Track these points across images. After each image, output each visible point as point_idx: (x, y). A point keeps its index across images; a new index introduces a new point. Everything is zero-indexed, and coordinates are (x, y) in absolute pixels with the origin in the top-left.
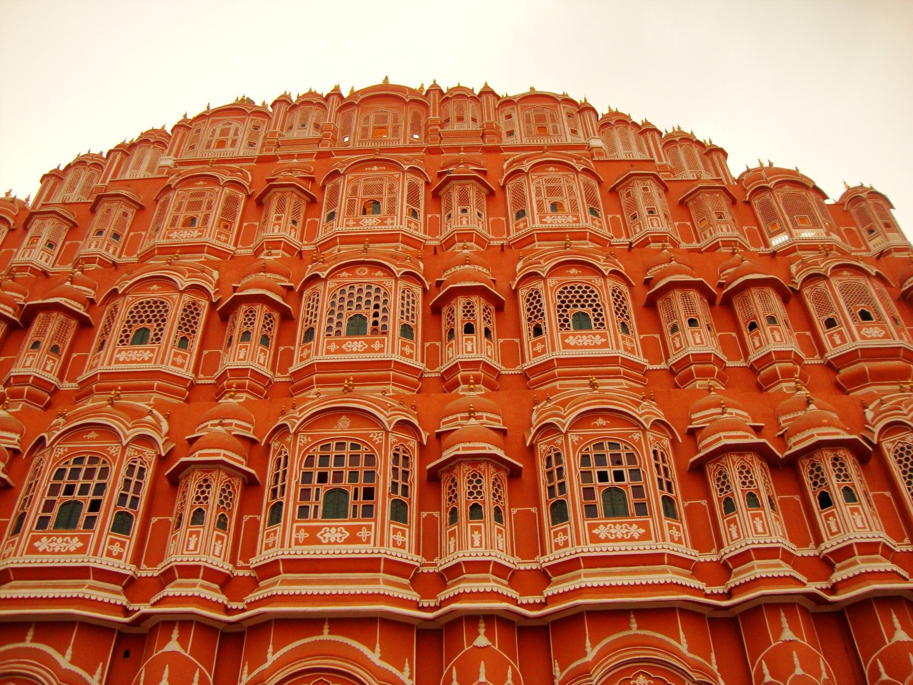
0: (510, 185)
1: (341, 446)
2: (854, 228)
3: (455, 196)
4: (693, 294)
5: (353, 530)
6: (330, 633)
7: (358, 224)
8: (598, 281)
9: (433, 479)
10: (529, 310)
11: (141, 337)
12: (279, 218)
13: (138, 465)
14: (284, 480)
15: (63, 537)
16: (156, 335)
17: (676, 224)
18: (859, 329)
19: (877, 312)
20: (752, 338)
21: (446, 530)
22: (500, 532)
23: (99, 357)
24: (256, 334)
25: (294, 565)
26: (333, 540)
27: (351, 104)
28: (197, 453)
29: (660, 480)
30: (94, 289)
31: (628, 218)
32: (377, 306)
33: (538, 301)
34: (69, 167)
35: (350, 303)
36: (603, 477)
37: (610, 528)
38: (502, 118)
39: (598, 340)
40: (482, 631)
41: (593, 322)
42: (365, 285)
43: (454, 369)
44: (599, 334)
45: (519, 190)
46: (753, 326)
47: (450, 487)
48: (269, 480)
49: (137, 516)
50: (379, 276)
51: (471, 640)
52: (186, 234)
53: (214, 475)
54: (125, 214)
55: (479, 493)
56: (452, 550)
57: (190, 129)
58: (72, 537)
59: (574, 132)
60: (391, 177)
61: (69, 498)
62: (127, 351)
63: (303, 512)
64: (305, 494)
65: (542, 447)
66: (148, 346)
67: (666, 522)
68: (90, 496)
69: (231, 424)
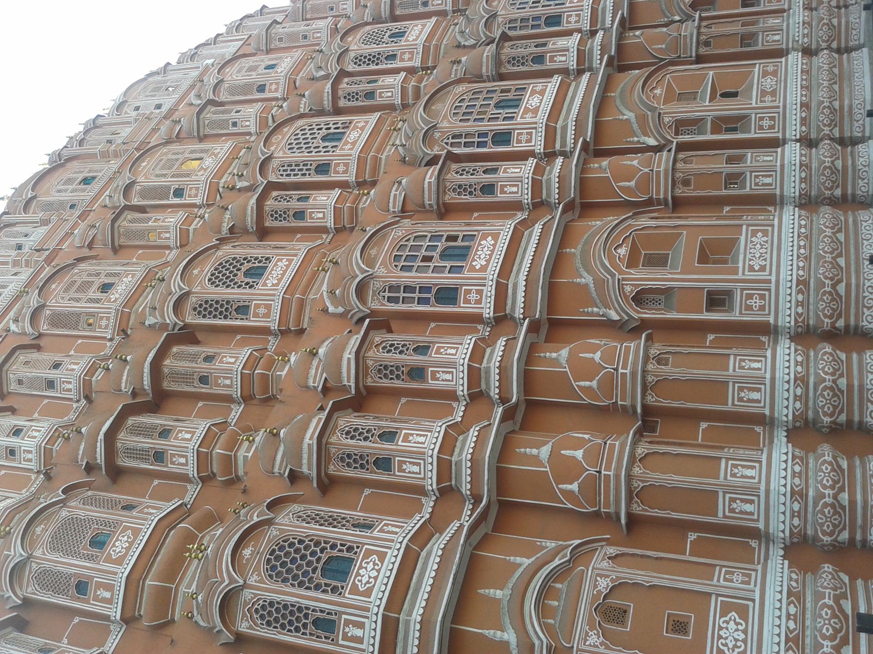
5: (533, 92)
7: (205, 170)
10: (368, 64)
16: (259, 262)
21: (549, 65)
23: (257, 306)
28: (427, 180)
31: (302, 42)
32: (319, 129)
43: (404, 90)
47: (513, 65)
51: (637, 37)
56: (564, 59)
58: (479, 244)
60: (166, 154)
62: (267, 279)
66: (271, 265)
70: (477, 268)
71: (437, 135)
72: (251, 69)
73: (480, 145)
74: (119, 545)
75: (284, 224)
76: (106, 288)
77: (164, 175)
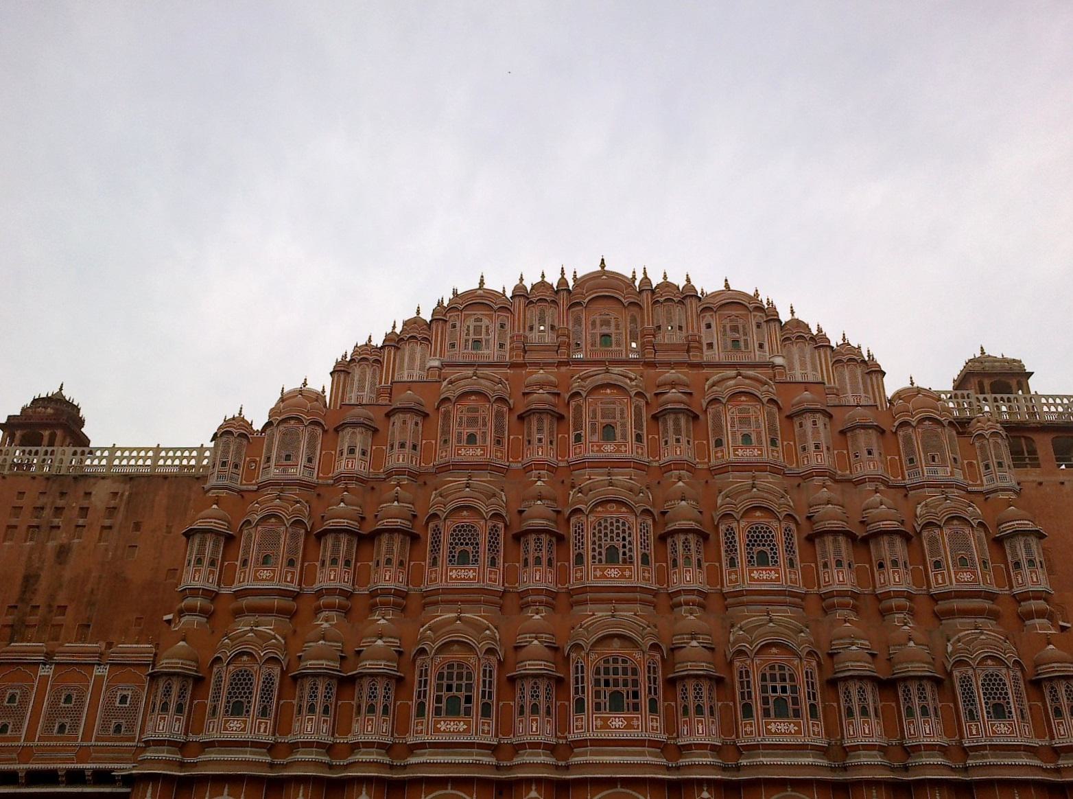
0: (710, 410)
1: (615, 661)
2: (975, 462)
3: (670, 423)
4: (841, 538)
6: (621, 787)
7: (600, 451)
8: (775, 524)
9: (671, 683)
10: (726, 543)
11: (463, 559)
13: (488, 669)
14: (582, 683)
15: (454, 721)
16: (474, 556)
17: (836, 452)
18: (956, 574)
19: (972, 559)
21: (682, 719)
22: (713, 722)
24: (545, 561)
25: (596, 742)
26: (617, 726)
27: (579, 304)
29: (809, 693)
30: (413, 504)
32: (624, 539)
33: (733, 537)
34: (352, 360)
35: (606, 535)
36: (774, 689)
38: (703, 326)
39: (773, 575)
40: (705, 789)
41: (770, 559)
42: (615, 519)
43: (678, 593)
45: (717, 417)
46: (881, 566)
48: (572, 681)
50: (624, 512)
52: (471, 452)
53: (540, 680)
54: (417, 424)
55: (701, 697)
57: (446, 321)
58: (460, 721)
59: (761, 346)
61: (451, 694)
63: (598, 707)
64: (598, 694)
65: (737, 664)
66: (470, 566)
68: (462, 694)
70: (439, 726)
71: (583, 654)
72: (745, 421)
73: (577, 689)
74: (265, 574)
75: (522, 553)
76: (472, 439)
77: (594, 417)
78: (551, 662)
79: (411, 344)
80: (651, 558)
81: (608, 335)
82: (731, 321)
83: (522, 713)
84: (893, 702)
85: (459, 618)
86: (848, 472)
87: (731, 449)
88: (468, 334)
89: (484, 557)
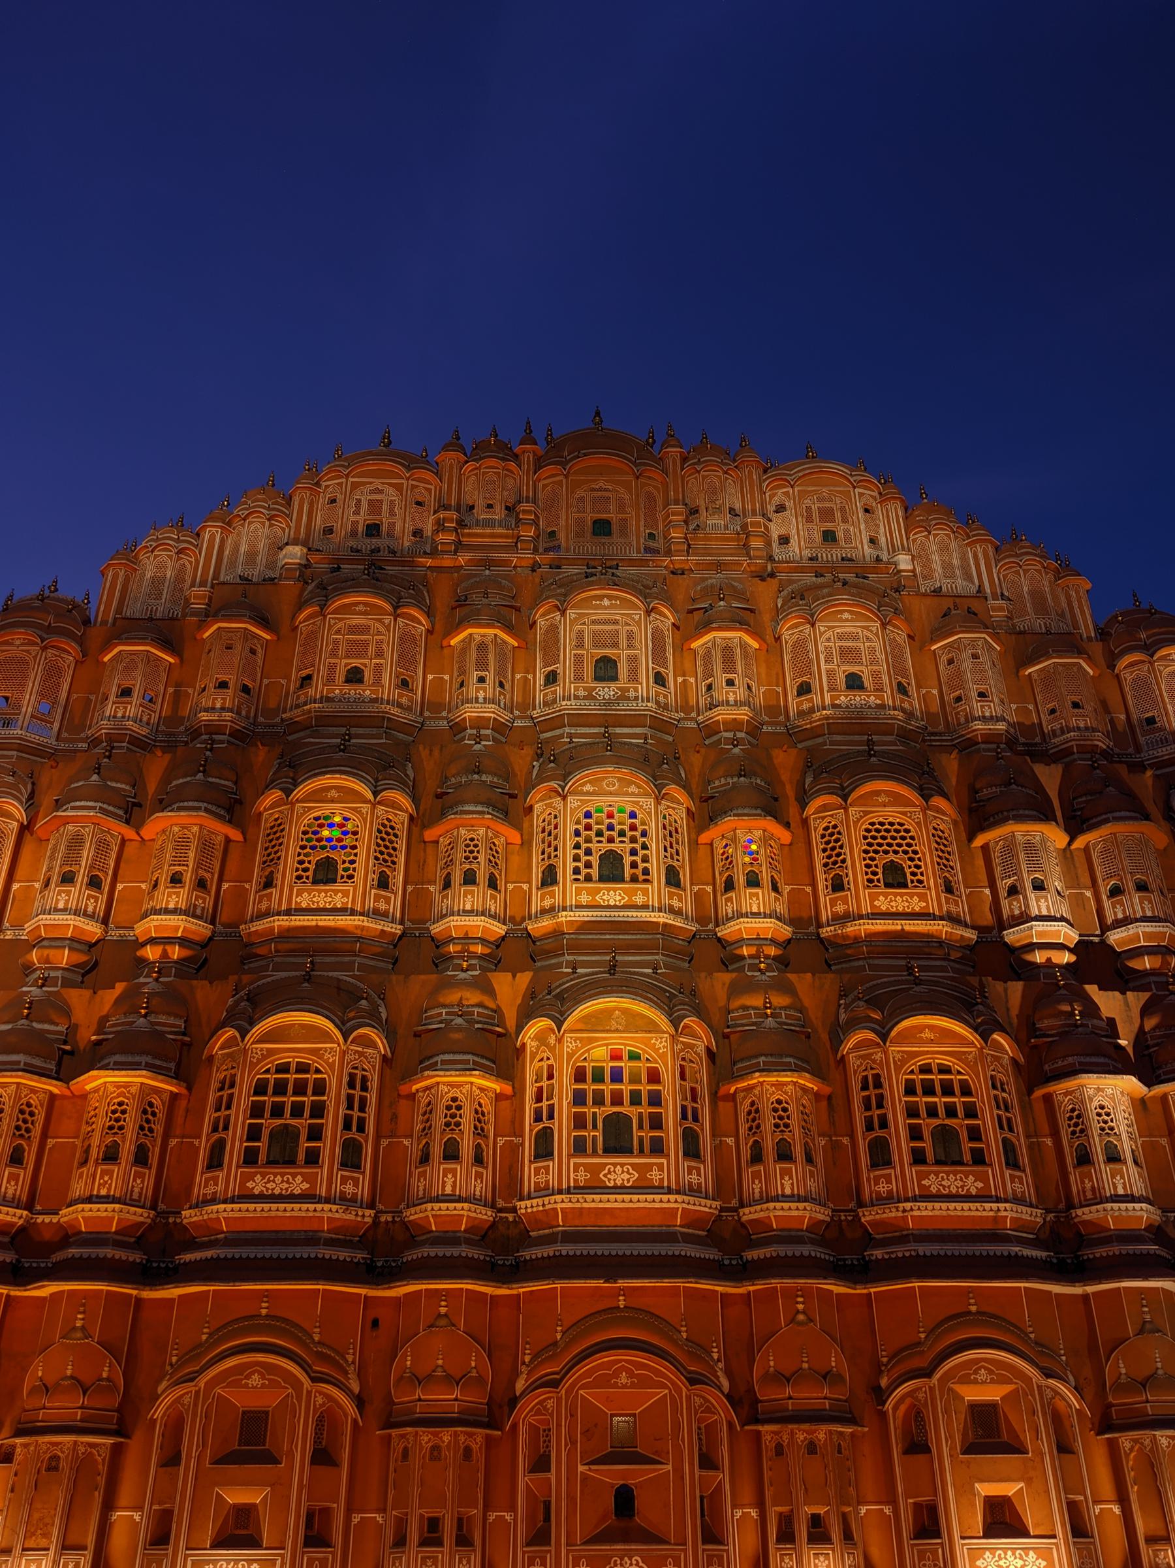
5: (642, 1169)
7: (589, 697)
11: (326, 873)
12: (481, 680)
17: (1014, 707)
20: (1114, 907)
22: (812, 1174)
24: (482, 876)
37: (943, 1179)
39: (917, 905)
41: (909, 877)
44: (918, 895)
45: (800, 646)
49: (366, 1142)
50: (633, 794)
58: (294, 1176)
63: (579, 1147)
64: (579, 1122)
67: (1007, 1173)
69: (472, 1013)
70: (250, 1184)
72: (849, 655)
78: (487, 1059)
79: (253, 527)
80: (684, 875)
81: (607, 523)
82: (820, 500)
83: (425, 1159)
84: (1161, 1136)
85: (308, 978)
86: (1038, 739)
87: (827, 696)
88: (357, 513)
89: (364, 865)
